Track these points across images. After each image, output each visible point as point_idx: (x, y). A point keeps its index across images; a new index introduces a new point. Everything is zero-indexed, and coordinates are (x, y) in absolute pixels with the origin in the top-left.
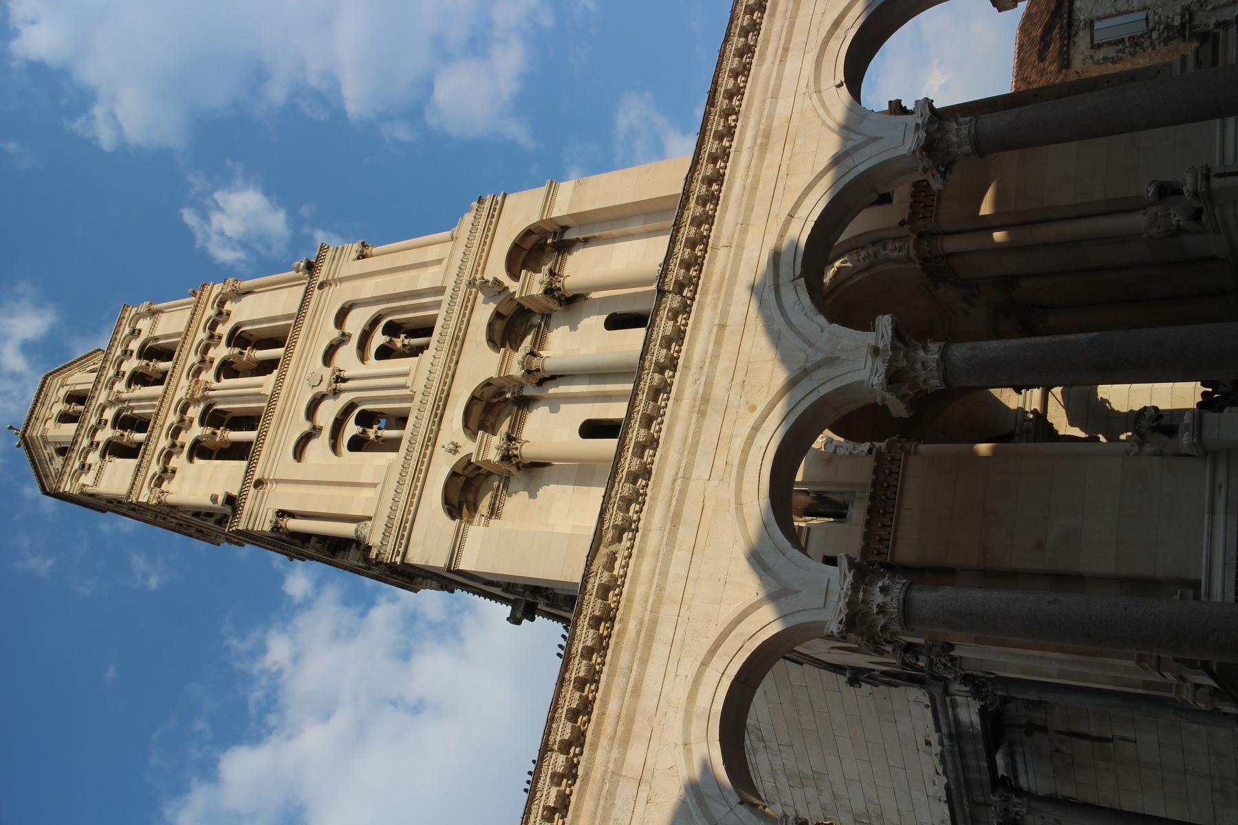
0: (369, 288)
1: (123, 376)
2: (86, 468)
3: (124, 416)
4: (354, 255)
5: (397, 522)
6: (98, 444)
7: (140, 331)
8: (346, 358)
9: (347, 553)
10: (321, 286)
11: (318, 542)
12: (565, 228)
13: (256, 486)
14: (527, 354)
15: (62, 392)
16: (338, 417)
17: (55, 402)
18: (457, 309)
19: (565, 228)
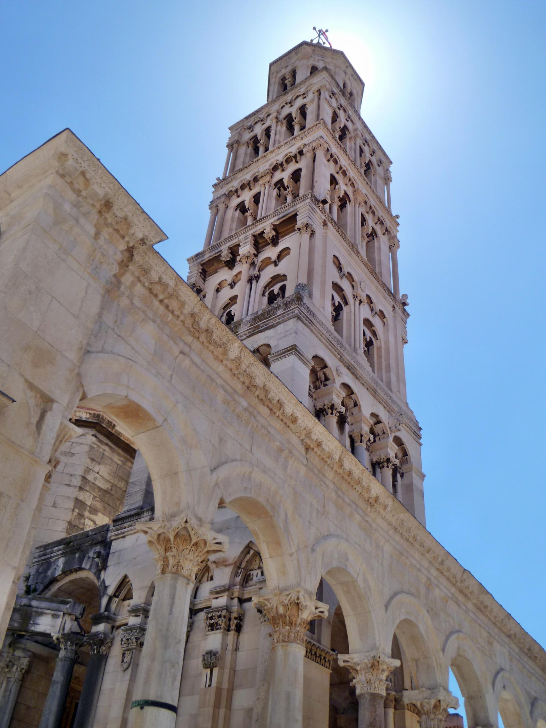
0: (392, 339)
1: (364, 144)
2: (332, 95)
3: (346, 134)
4: (404, 335)
5: (312, 319)
6: (339, 109)
7: (379, 166)
8: (365, 312)
9: (253, 246)
10: (394, 307)
11: (273, 236)
12: (402, 476)
13: (325, 220)
14: (370, 438)
15: (355, 92)
16: (343, 292)
17: (352, 84)
18: (385, 397)
19: (402, 476)
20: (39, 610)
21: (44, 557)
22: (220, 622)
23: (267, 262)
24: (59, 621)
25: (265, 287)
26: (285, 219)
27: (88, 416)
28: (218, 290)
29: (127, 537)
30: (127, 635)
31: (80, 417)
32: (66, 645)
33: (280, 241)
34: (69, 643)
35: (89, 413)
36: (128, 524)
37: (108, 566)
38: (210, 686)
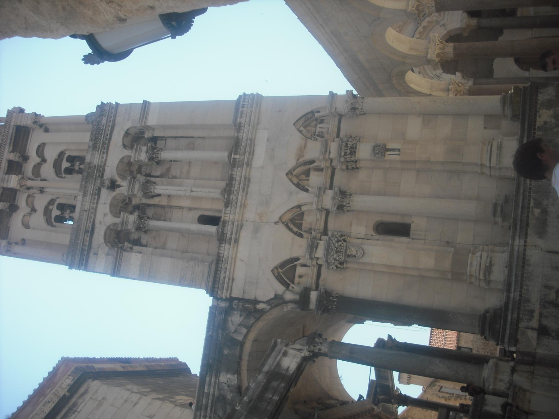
20: (275, 364)
21: (209, 409)
22: (351, 144)
23: (37, 169)
24: (291, 352)
25: (57, 175)
26: (13, 141)
27: (71, 378)
28: (27, 226)
29: (235, 276)
30: (332, 253)
31: (68, 385)
32: (318, 343)
33: (26, 155)
34: (316, 339)
35: (70, 375)
36: (223, 272)
37: (255, 298)
38: (399, 150)
